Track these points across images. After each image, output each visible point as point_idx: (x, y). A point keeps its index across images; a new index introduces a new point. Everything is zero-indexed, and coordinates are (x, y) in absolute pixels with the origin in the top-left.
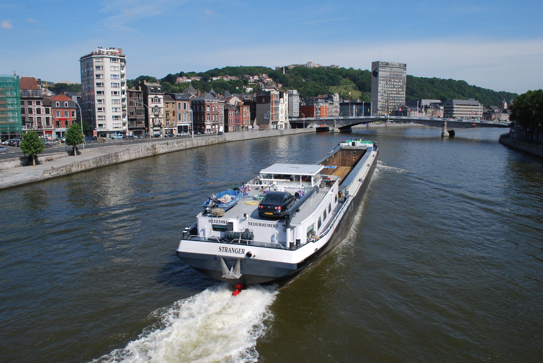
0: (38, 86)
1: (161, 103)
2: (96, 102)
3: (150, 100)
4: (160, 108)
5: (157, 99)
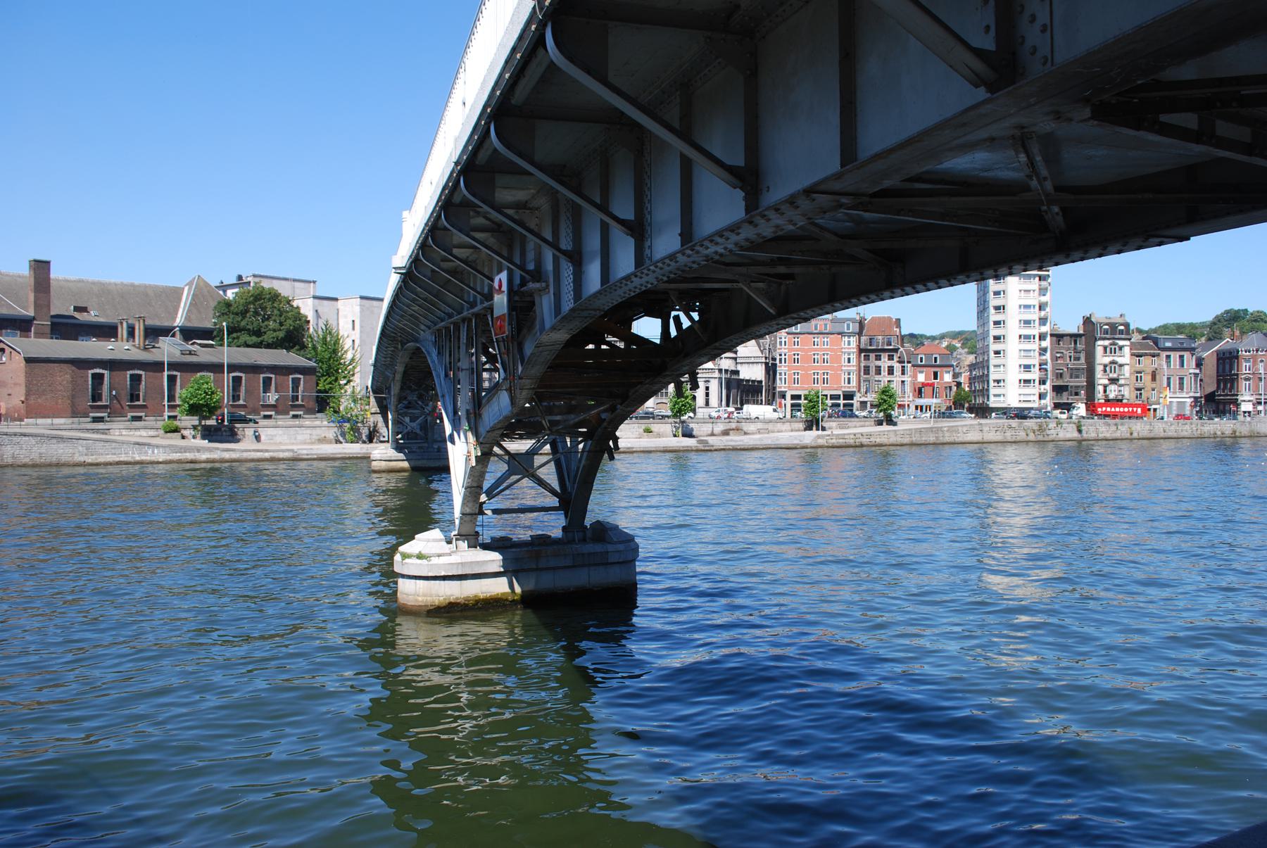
1: (1124, 356)
2: (992, 355)
3: (1099, 351)
4: (1121, 366)
5: (1115, 349)
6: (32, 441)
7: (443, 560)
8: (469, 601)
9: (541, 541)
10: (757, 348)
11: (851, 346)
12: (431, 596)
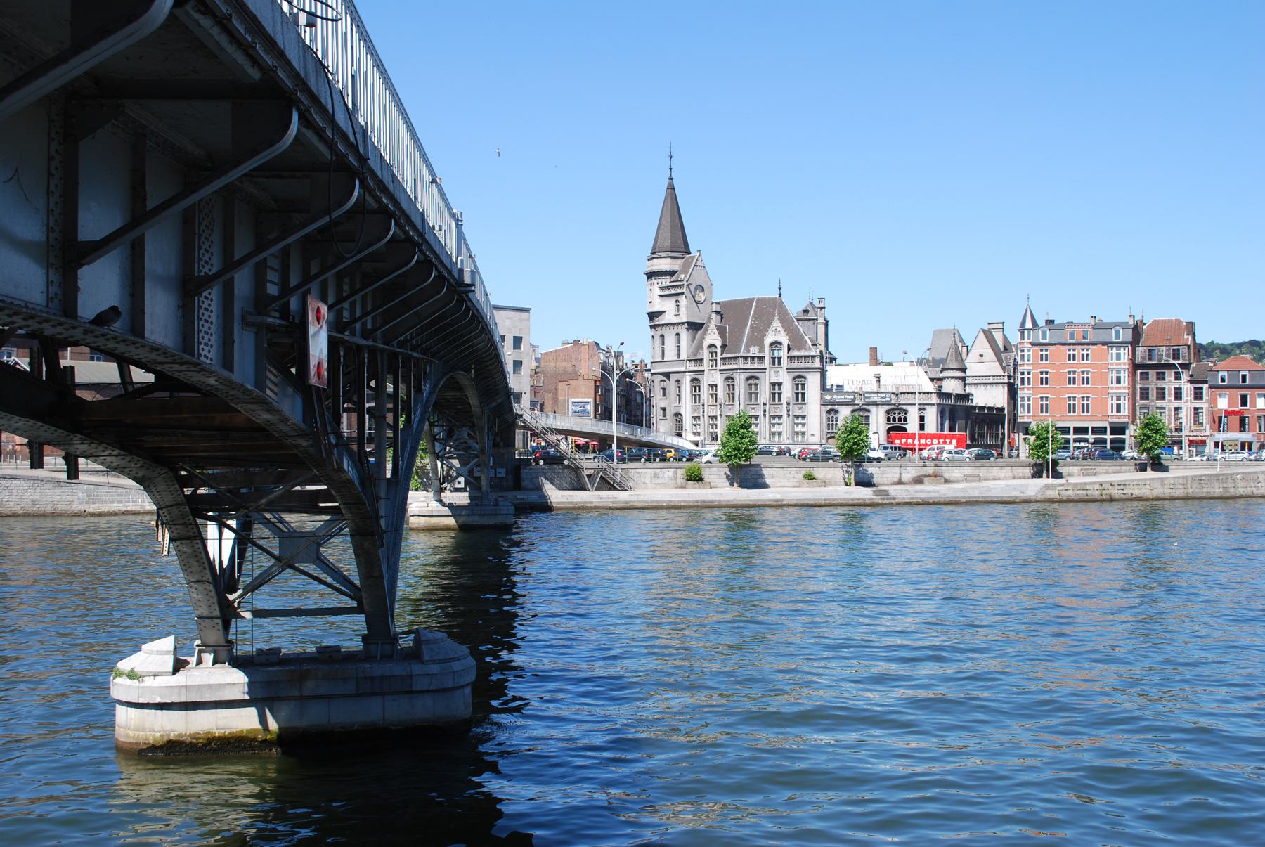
0: (1186, 337)
6: (24, 484)
7: (160, 681)
8: (197, 739)
9: (328, 655)
10: (997, 363)
11: (1122, 361)
12: (144, 730)
